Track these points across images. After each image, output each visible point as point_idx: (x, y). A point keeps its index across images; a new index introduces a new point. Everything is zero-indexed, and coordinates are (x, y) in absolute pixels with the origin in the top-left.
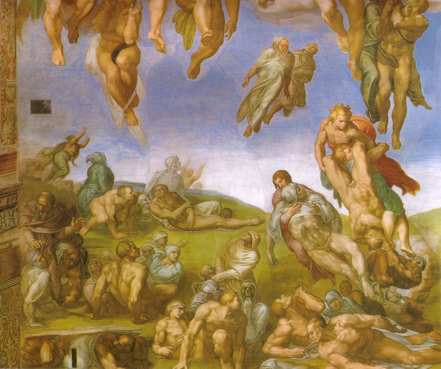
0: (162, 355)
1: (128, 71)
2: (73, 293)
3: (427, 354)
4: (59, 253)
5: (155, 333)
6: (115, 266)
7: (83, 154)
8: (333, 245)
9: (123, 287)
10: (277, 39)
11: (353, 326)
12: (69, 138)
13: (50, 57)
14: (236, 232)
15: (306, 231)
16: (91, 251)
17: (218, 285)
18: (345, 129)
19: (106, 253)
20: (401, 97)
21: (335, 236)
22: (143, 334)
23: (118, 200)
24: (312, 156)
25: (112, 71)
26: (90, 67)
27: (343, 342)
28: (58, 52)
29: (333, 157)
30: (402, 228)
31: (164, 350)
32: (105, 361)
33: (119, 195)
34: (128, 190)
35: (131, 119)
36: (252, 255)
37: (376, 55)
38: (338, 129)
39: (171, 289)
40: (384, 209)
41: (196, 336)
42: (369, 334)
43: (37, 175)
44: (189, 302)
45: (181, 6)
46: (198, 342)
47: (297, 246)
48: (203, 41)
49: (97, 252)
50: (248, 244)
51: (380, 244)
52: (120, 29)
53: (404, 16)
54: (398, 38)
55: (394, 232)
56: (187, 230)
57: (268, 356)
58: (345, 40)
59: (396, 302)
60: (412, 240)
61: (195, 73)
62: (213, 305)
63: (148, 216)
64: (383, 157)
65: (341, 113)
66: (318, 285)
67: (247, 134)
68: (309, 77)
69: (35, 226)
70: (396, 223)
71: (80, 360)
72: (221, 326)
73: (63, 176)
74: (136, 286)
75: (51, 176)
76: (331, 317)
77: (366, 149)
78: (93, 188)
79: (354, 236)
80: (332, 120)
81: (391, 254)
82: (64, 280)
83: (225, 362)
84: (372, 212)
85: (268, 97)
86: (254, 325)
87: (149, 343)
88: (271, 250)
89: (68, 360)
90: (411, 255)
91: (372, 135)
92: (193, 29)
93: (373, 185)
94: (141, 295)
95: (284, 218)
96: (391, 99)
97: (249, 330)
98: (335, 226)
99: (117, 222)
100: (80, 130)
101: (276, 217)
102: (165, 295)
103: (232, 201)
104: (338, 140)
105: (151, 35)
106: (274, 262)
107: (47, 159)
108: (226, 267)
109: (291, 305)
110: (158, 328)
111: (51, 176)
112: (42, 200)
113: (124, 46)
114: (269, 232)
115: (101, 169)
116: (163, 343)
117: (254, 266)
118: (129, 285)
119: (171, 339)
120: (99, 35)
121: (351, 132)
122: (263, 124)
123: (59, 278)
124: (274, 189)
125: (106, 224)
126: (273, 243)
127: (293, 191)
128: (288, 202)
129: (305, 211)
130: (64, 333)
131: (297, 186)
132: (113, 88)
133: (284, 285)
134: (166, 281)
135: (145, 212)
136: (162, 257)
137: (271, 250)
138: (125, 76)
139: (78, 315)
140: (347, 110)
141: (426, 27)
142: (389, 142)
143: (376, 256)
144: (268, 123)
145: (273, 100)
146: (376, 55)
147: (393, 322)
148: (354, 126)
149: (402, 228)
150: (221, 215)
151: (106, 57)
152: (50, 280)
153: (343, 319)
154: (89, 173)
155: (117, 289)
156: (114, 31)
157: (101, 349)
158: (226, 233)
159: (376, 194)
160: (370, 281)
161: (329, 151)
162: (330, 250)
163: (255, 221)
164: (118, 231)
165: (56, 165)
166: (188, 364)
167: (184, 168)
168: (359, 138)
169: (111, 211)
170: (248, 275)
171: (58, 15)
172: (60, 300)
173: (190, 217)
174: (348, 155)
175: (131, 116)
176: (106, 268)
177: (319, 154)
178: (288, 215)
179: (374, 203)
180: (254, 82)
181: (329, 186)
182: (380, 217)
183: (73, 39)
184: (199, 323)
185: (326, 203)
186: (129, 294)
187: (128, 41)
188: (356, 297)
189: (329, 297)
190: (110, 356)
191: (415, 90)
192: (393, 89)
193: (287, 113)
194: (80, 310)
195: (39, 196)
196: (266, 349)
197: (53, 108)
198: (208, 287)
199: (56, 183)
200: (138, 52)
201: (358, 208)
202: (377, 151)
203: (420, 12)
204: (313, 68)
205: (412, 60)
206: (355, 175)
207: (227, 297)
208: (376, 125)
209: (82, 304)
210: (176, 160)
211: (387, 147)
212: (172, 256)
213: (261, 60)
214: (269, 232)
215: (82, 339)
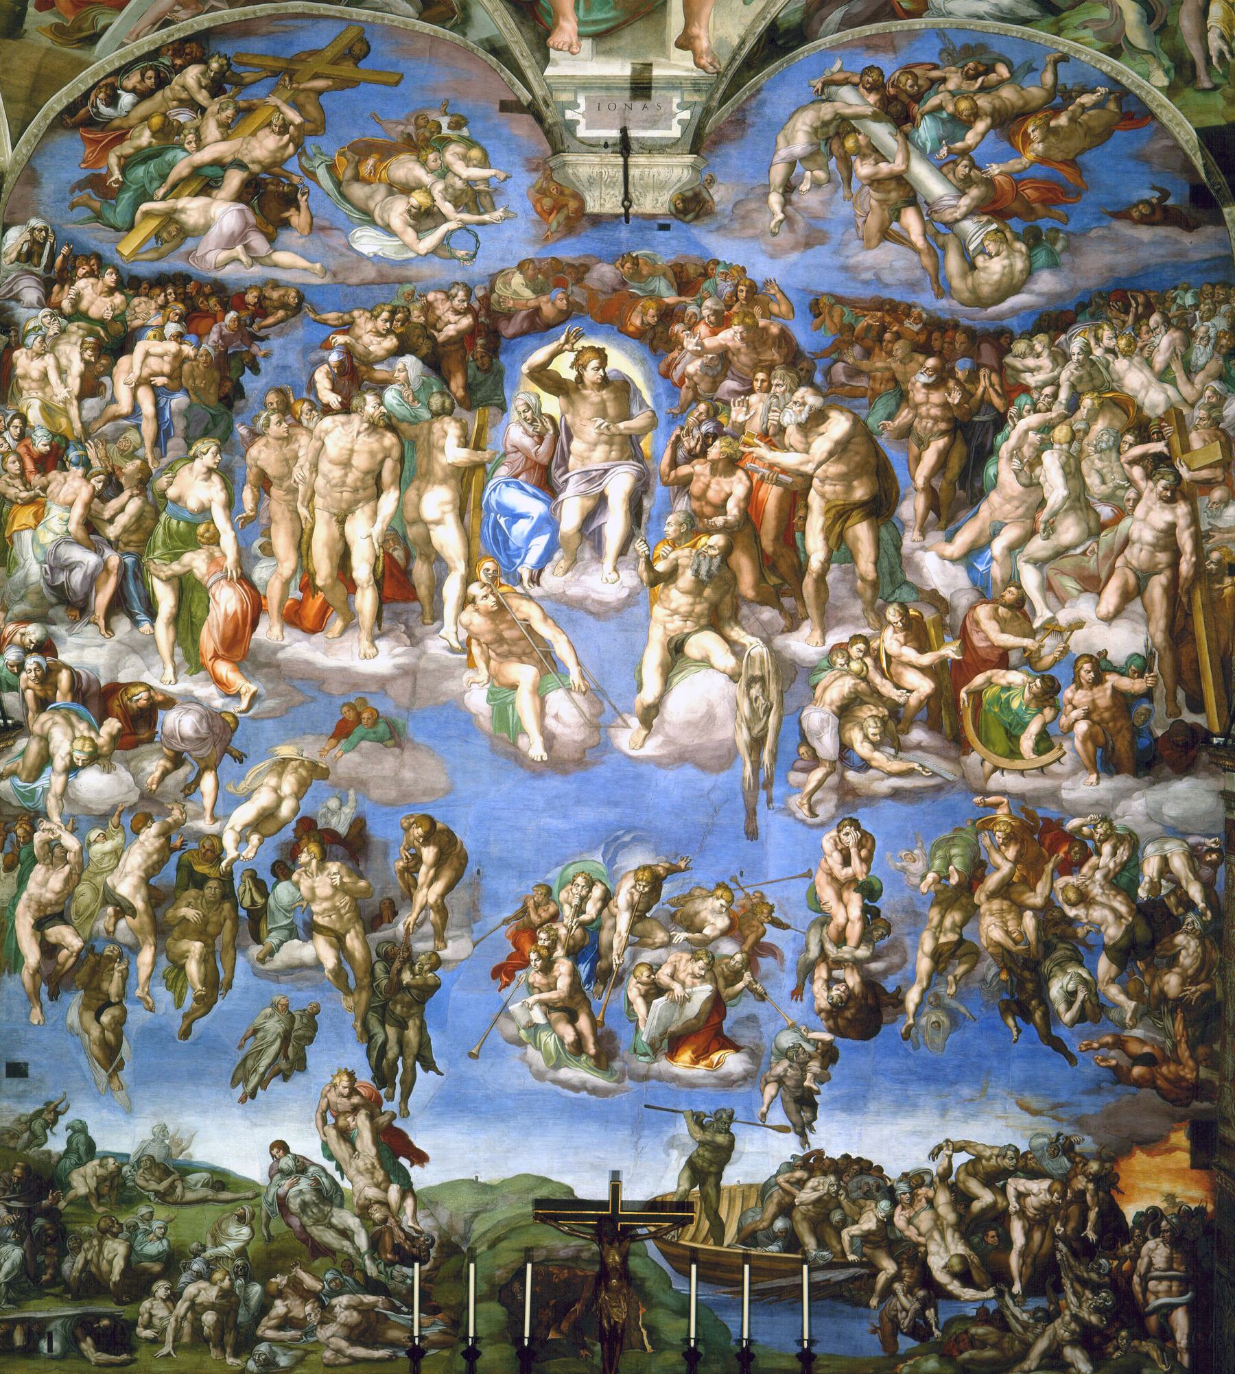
0: (147, 1339)
1: (113, 1031)
2: (50, 1271)
3: (433, 1338)
4: (34, 1228)
5: (139, 1314)
6: (95, 1242)
7: (63, 1121)
8: (334, 1221)
9: (104, 1266)
10: (276, 998)
11: (354, 1308)
12: (48, 1104)
13: (28, 1015)
14: (228, 1207)
15: (304, 1205)
16: (70, 1227)
17: (208, 1263)
18: (349, 1096)
19: (86, 1229)
20: (410, 1061)
21: (336, 1210)
22: (126, 1316)
23: (100, 1172)
24: (313, 1124)
25: (95, 1031)
26: (72, 1027)
27: (344, 1325)
28: (37, 1011)
29: (336, 1126)
30: (409, 1202)
31: (148, 1333)
32: (83, 1346)
33: (101, 1166)
34: (111, 1161)
35: (115, 1083)
36: (246, 1231)
37: (383, 1016)
38: (342, 1095)
39: (157, 1268)
40: (391, 1182)
41: (184, 1317)
42: (373, 1316)
43: (12, 1144)
44: (177, 1281)
45: (172, 961)
46: (186, 1324)
47: (295, 1222)
48: (196, 999)
49: (77, 1228)
50: (241, 1219)
51: (385, 1220)
52: (105, 985)
53: (414, 974)
54: (408, 998)
55: (401, 1207)
56: (175, 1203)
57: (262, 1340)
58: (350, 999)
59: (403, 1282)
60: (420, 1215)
61: (186, 1033)
62: (203, 1284)
63: (132, 1189)
64: (390, 1126)
65: (345, 1078)
66: (317, 1263)
67: (242, 1100)
68: (310, 1040)
69: (9, 1200)
70: (403, 1198)
71: (56, 1345)
72: (212, 1307)
73: (41, 1145)
74: (119, 1264)
75: (28, 1145)
76: (331, 1297)
77: (372, 1117)
78: (73, 1158)
79: (357, 1210)
80: (335, 1086)
81: (396, 1230)
82: (40, 1258)
83: (215, 1346)
84: (377, 1186)
85: (265, 1061)
86: (247, 1306)
87: (135, 1324)
88: (267, 1226)
89: (44, 1345)
90: (420, 1232)
91: (379, 1103)
92: (184, 987)
93: (379, 1156)
94: (123, 1273)
95: (281, 1191)
96: (400, 1063)
97: (242, 1311)
98: (337, 1201)
99: (98, 1194)
100: (60, 1095)
101: (273, 1190)
102: (151, 1274)
103: (224, 1173)
104: (341, 1108)
105: (139, 993)
106: (270, 1238)
107: (24, 1127)
108: (217, 1244)
109: (287, 1285)
110: (142, 1309)
111: (28, 1145)
112: (17, 1171)
113: (109, 1004)
114: (264, 1206)
115: (82, 1138)
116: (149, 1325)
117: (248, 1242)
118: (110, 1263)
119: (156, 1321)
120: (82, 992)
121: (356, 1100)
122: (259, 1091)
123: (34, 1256)
124: (271, 1161)
125: (86, 1198)
126: (269, 1218)
127: (291, 1163)
128: (285, 1174)
129: (304, 1184)
130: (40, 1315)
131: (295, 1157)
132: (96, 1050)
133: (280, 1263)
134: (151, 1258)
135: (130, 1184)
136: (147, 1233)
137: (267, 1226)
138: (110, 1036)
139: (56, 1296)
140: (351, 1076)
141: (438, 986)
142: (396, 1111)
143: (381, 1233)
144: (265, 1088)
145: (270, 1065)
146: (383, 1016)
147: (398, 1303)
148: (359, 1093)
149: (409, 1202)
150: (213, 1188)
151: (89, 1016)
152: (24, 1256)
153: (344, 1300)
154: (69, 1142)
155: (98, 1267)
156: (98, 988)
157: (79, 1332)
158: (220, 1207)
159: (382, 1166)
160: (373, 1259)
161: (331, 1120)
162: (332, 1226)
163: (249, 1194)
164: (99, 1205)
165: (33, 1133)
166: (174, 1348)
167: (173, 1137)
168: (363, 1106)
169: (93, 1183)
170: (241, 1252)
171: (37, 971)
172: (36, 1279)
173: (179, 1190)
174: (352, 1124)
175: (115, 1080)
176: (86, 1245)
177: (320, 1123)
178: (286, 1188)
179: (380, 1175)
180: (250, 1045)
181: (330, 1157)
182: (386, 1190)
183: (53, 996)
184: (187, 1304)
185: (328, 1175)
186: (111, 1272)
187: (114, 999)
188: (358, 1276)
189: (329, 1276)
190: (89, 1340)
191: (426, 1054)
192: (401, 1052)
193: (286, 1078)
194: (57, 1290)
195: (15, 1166)
196: (259, 1333)
197: (32, 1071)
198: (197, 1266)
199: (32, 1152)
200: (125, 1012)
201: (362, 1181)
202: (383, 1120)
203: (432, 970)
204: (315, 1030)
205: (422, 1022)
206: (358, 1145)
207: (217, 1276)
208: (382, 1092)
209: (59, 1284)
210: (164, 1128)
211: (394, 1116)
212: (159, 1232)
213: (259, 1020)
214: (264, 1206)
215: (59, 1322)
